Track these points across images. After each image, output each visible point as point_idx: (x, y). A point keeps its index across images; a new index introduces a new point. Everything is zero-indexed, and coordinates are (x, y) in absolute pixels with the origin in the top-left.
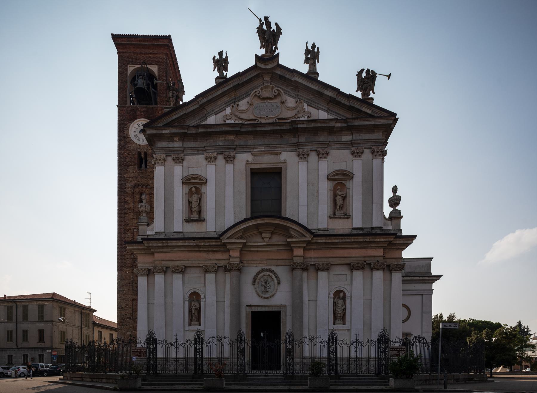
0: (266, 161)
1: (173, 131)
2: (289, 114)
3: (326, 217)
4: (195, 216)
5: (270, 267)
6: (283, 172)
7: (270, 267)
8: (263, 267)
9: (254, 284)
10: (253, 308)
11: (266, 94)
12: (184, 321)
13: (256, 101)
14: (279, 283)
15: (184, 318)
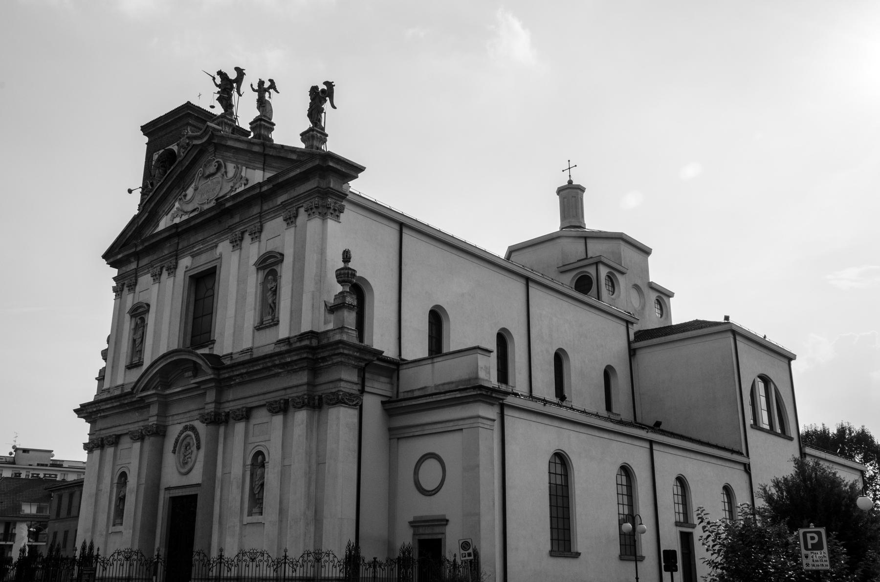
0: (203, 262)
1: (126, 253)
2: (227, 188)
3: (251, 329)
4: (136, 360)
5: (191, 423)
6: (218, 272)
7: (191, 423)
8: (184, 425)
9: (174, 452)
10: (171, 492)
11: (212, 169)
12: (108, 518)
13: (203, 182)
14: (198, 448)
15: (109, 513)
